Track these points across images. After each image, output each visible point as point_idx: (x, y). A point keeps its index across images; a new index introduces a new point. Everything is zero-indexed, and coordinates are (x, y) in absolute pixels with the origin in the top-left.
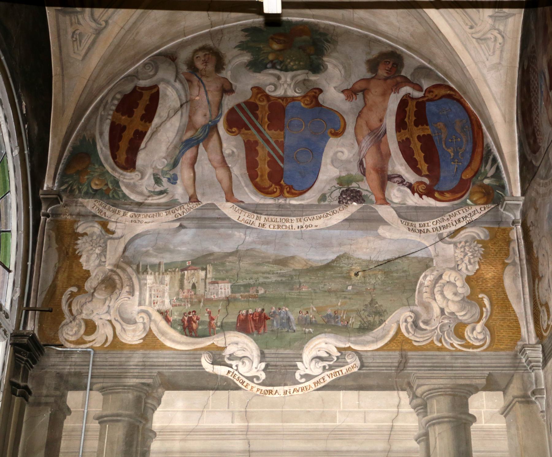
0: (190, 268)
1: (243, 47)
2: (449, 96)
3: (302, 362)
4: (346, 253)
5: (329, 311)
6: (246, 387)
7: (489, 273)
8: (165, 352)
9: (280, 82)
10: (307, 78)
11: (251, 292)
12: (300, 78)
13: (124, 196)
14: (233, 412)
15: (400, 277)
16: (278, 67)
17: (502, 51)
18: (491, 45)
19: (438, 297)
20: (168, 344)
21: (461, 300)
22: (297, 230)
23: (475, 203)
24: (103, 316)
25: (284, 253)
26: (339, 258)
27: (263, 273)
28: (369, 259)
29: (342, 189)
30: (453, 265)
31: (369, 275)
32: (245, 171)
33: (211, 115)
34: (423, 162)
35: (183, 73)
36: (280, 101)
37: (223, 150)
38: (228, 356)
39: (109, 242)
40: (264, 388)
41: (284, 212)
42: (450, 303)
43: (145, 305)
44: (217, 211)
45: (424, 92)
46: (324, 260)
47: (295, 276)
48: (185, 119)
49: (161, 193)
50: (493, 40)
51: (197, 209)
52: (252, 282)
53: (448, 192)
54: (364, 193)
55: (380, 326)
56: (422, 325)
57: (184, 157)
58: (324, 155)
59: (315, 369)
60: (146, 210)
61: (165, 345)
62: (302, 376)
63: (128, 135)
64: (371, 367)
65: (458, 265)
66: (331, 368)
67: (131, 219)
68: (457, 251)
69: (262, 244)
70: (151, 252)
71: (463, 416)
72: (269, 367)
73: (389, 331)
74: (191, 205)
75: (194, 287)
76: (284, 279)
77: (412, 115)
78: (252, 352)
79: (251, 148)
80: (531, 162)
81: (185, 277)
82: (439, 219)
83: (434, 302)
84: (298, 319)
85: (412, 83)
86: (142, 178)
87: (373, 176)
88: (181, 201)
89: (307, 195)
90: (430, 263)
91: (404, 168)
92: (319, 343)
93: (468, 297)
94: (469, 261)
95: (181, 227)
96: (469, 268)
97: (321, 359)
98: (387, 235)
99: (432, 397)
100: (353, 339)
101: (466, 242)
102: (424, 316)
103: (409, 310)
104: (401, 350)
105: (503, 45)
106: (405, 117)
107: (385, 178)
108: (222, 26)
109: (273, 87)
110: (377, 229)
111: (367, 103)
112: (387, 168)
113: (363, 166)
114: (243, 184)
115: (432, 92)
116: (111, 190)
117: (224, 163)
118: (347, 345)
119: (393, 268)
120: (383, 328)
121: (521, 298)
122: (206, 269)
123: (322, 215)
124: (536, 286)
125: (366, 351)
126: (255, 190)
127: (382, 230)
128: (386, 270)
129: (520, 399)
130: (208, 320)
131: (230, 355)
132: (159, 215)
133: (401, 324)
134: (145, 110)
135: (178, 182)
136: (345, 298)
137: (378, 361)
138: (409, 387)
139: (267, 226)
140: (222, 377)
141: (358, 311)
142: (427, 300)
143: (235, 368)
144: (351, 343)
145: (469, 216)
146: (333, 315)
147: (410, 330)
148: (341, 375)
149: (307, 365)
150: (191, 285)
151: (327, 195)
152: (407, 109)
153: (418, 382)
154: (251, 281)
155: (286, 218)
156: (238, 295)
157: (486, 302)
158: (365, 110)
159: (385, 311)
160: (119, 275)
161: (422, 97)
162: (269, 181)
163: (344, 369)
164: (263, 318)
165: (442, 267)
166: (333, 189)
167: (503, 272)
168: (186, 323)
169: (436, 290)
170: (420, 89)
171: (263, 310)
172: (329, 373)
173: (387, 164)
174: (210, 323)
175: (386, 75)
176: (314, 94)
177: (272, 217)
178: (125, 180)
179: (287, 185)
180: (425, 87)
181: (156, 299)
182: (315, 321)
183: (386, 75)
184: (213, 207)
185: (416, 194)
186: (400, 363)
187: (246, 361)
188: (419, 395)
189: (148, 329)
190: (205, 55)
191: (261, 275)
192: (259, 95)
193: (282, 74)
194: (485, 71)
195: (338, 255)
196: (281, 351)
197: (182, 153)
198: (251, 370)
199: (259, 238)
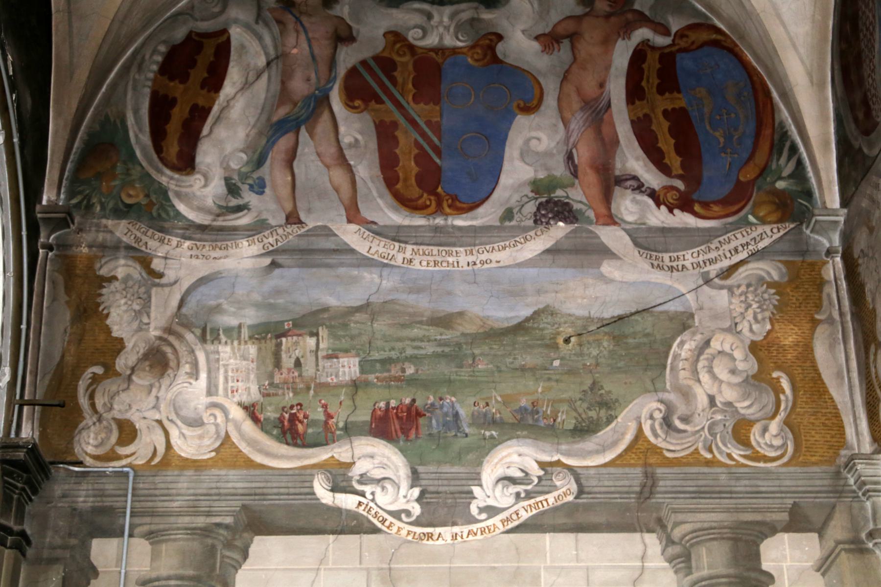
0: (290, 333)
2: (715, 43)
3: (481, 486)
4: (548, 306)
5: (524, 402)
6: (388, 528)
7: (789, 337)
9: (432, 23)
10: (476, 16)
11: (393, 372)
12: (465, 16)
14: (368, 570)
15: (641, 344)
19: (705, 377)
20: (259, 459)
21: (743, 381)
22: (466, 268)
23: (763, 221)
24: (147, 414)
25: (447, 307)
26: (537, 313)
27: (413, 340)
28: (587, 315)
29: (540, 200)
30: (727, 324)
31: (589, 343)
32: (377, 171)
33: (318, 79)
34: (673, 154)
36: (432, 54)
37: (340, 137)
38: (358, 478)
39: (154, 291)
40: (419, 530)
41: (445, 239)
42: (724, 386)
44: (333, 238)
45: (672, 38)
46: (512, 318)
47: (466, 343)
48: (276, 87)
49: (239, 209)
51: (299, 236)
52: (394, 354)
53: (716, 203)
54: (576, 206)
55: (608, 425)
56: (678, 424)
57: (275, 148)
58: (507, 143)
59: (503, 497)
60: (214, 237)
61: (252, 461)
62: (481, 510)
63: (179, 114)
64: (596, 493)
65: (736, 324)
66: (529, 495)
68: (734, 301)
69: (410, 293)
70: (225, 306)
71: (753, 575)
72: (427, 496)
73: (623, 434)
74: (289, 229)
75: (298, 364)
76: (447, 350)
77: (654, 75)
78: (398, 471)
79: (385, 134)
80: (860, 149)
81: (283, 347)
82: (703, 247)
83: (698, 384)
84: (473, 415)
86: (205, 186)
87: (590, 177)
88: (272, 222)
89: (481, 210)
90: (690, 322)
91: (641, 163)
92: (509, 455)
93: (754, 377)
94: (755, 318)
95: (274, 265)
96: (755, 328)
97: (512, 481)
98: (617, 275)
99: (698, 543)
100: (564, 447)
101: (748, 286)
102: (682, 409)
103: (656, 398)
104: (646, 465)
106: (642, 79)
107: (610, 182)
109: (420, 31)
110: (599, 265)
111: (577, 56)
112: (614, 165)
113: (573, 161)
114: (375, 194)
115: (687, 36)
116: (154, 204)
118: (555, 458)
119: (628, 330)
120: (614, 430)
121: (843, 378)
122: (317, 335)
123: (507, 243)
124: (872, 357)
125: (587, 467)
127: (607, 268)
128: (617, 333)
129: (847, 546)
130: (322, 417)
131: (362, 475)
132: (237, 246)
133: (643, 421)
134: (208, 73)
135: (267, 190)
136: (549, 379)
137: (606, 483)
138: (659, 525)
139: (416, 262)
141: (571, 402)
142: (686, 382)
143: (371, 497)
144: (562, 454)
145: (753, 243)
146: (530, 408)
147: (659, 431)
148: (546, 507)
149: (488, 492)
150: (293, 360)
151: (515, 211)
152: (645, 66)
153: (673, 518)
154: (393, 353)
155: (447, 249)
156: (371, 377)
157: (785, 384)
158: (575, 68)
159: (617, 401)
162: (417, 189)
163: (551, 498)
164: (414, 413)
165: (709, 327)
166: (525, 199)
168: (286, 423)
169: (700, 365)
170: (666, 32)
171: (414, 401)
172: (525, 503)
173: (614, 158)
174: (326, 423)
175: (608, 9)
176: (489, 43)
177: (425, 247)
179: (448, 195)
180: (674, 29)
181: (235, 384)
182: (501, 418)
183: (608, 9)
184: (326, 232)
185: (663, 207)
186: (643, 486)
188: (676, 540)
189: (223, 434)
191: (409, 343)
192: (398, 45)
195: (536, 308)
196: (446, 468)
197: (271, 142)
198: (395, 500)
199: (404, 283)
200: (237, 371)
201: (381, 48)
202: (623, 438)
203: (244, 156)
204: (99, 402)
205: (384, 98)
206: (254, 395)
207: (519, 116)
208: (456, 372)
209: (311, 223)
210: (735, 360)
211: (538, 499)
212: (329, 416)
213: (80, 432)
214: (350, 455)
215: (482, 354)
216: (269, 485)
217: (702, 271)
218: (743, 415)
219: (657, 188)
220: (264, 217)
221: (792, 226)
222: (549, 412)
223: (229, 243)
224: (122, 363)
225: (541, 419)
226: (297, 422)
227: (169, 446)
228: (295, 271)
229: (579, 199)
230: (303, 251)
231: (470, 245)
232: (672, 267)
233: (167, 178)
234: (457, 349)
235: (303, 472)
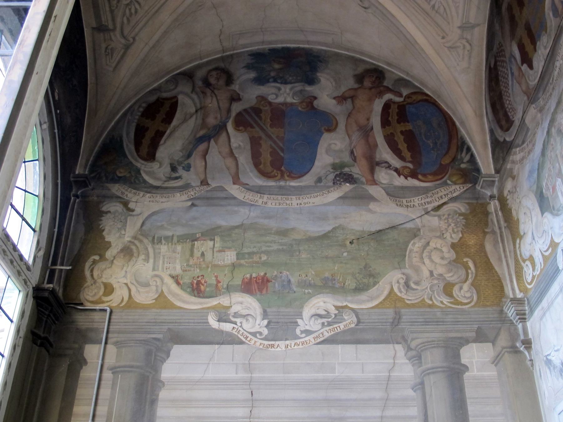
1: (249, 67)
3: (302, 319)
4: (341, 225)
5: (327, 275)
6: (249, 341)
7: (472, 241)
8: (175, 311)
13: (145, 181)
16: (279, 81)
17: (470, 57)
19: (427, 261)
20: (179, 304)
22: (296, 206)
23: (455, 183)
24: (120, 280)
27: (266, 242)
30: (438, 234)
33: (221, 118)
34: (406, 151)
36: (281, 106)
37: (231, 144)
40: (266, 343)
41: (284, 192)
43: (158, 270)
48: (200, 121)
49: (176, 178)
50: (462, 47)
51: (207, 191)
52: (255, 250)
53: (430, 174)
54: (355, 176)
56: (413, 285)
57: (197, 149)
59: (315, 325)
61: (175, 305)
62: (302, 332)
66: (329, 324)
67: (150, 199)
68: (441, 222)
70: (165, 226)
73: (383, 291)
74: (202, 188)
75: (203, 254)
76: (285, 247)
78: (256, 311)
80: (505, 140)
81: (195, 246)
82: (424, 196)
86: (160, 167)
87: (363, 163)
88: (193, 184)
89: (305, 178)
90: (418, 233)
92: (318, 302)
93: (454, 261)
94: (453, 231)
95: (193, 205)
97: (320, 316)
98: (378, 209)
99: (426, 349)
100: (349, 298)
101: (449, 215)
102: (414, 277)
108: (232, 52)
113: (354, 155)
114: (248, 170)
115: (411, 97)
117: (231, 154)
118: (345, 304)
121: (501, 261)
122: (214, 240)
123: (319, 194)
124: (517, 246)
126: (259, 175)
127: (372, 206)
130: (215, 283)
131: (235, 313)
135: (191, 169)
136: (341, 263)
137: (373, 317)
138: (404, 340)
140: (227, 332)
143: (240, 325)
144: (348, 302)
146: (330, 277)
147: (402, 290)
149: (306, 322)
150: (200, 253)
151: (323, 178)
154: (255, 249)
157: (471, 264)
159: (379, 274)
161: (402, 102)
163: (342, 326)
164: (265, 280)
168: (195, 285)
169: (424, 255)
170: (400, 95)
171: (266, 274)
172: (327, 328)
174: (217, 285)
175: (370, 85)
177: (274, 196)
178: (146, 169)
180: (404, 94)
181: (168, 265)
183: (370, 85)
184: (222, 189)
185: (402, 176)
186: (394, 319)
187: (250, 318)
189: (160, 291)
190: (217, 74)
192: (263, 102)
193: (282, 87)
195: (334, 226)
196: (283, 309)
197: (195, 147)
198: (253, 327)
203: (181, 154)
204: (96, 274)
205: (255, 125)
209: (214, 184)
210: (443, 252)
212: (219, 282)
213: (84, 289)
214: (229, 302)
216: (184, 318)
220: (189, 182)
221: (470, 185)
223: (170, 195)
224: (109, 254)
227: (130, 296)
228: (203, 208)
230: (208, 198)
231: (299, 195)
233: (139, 164)
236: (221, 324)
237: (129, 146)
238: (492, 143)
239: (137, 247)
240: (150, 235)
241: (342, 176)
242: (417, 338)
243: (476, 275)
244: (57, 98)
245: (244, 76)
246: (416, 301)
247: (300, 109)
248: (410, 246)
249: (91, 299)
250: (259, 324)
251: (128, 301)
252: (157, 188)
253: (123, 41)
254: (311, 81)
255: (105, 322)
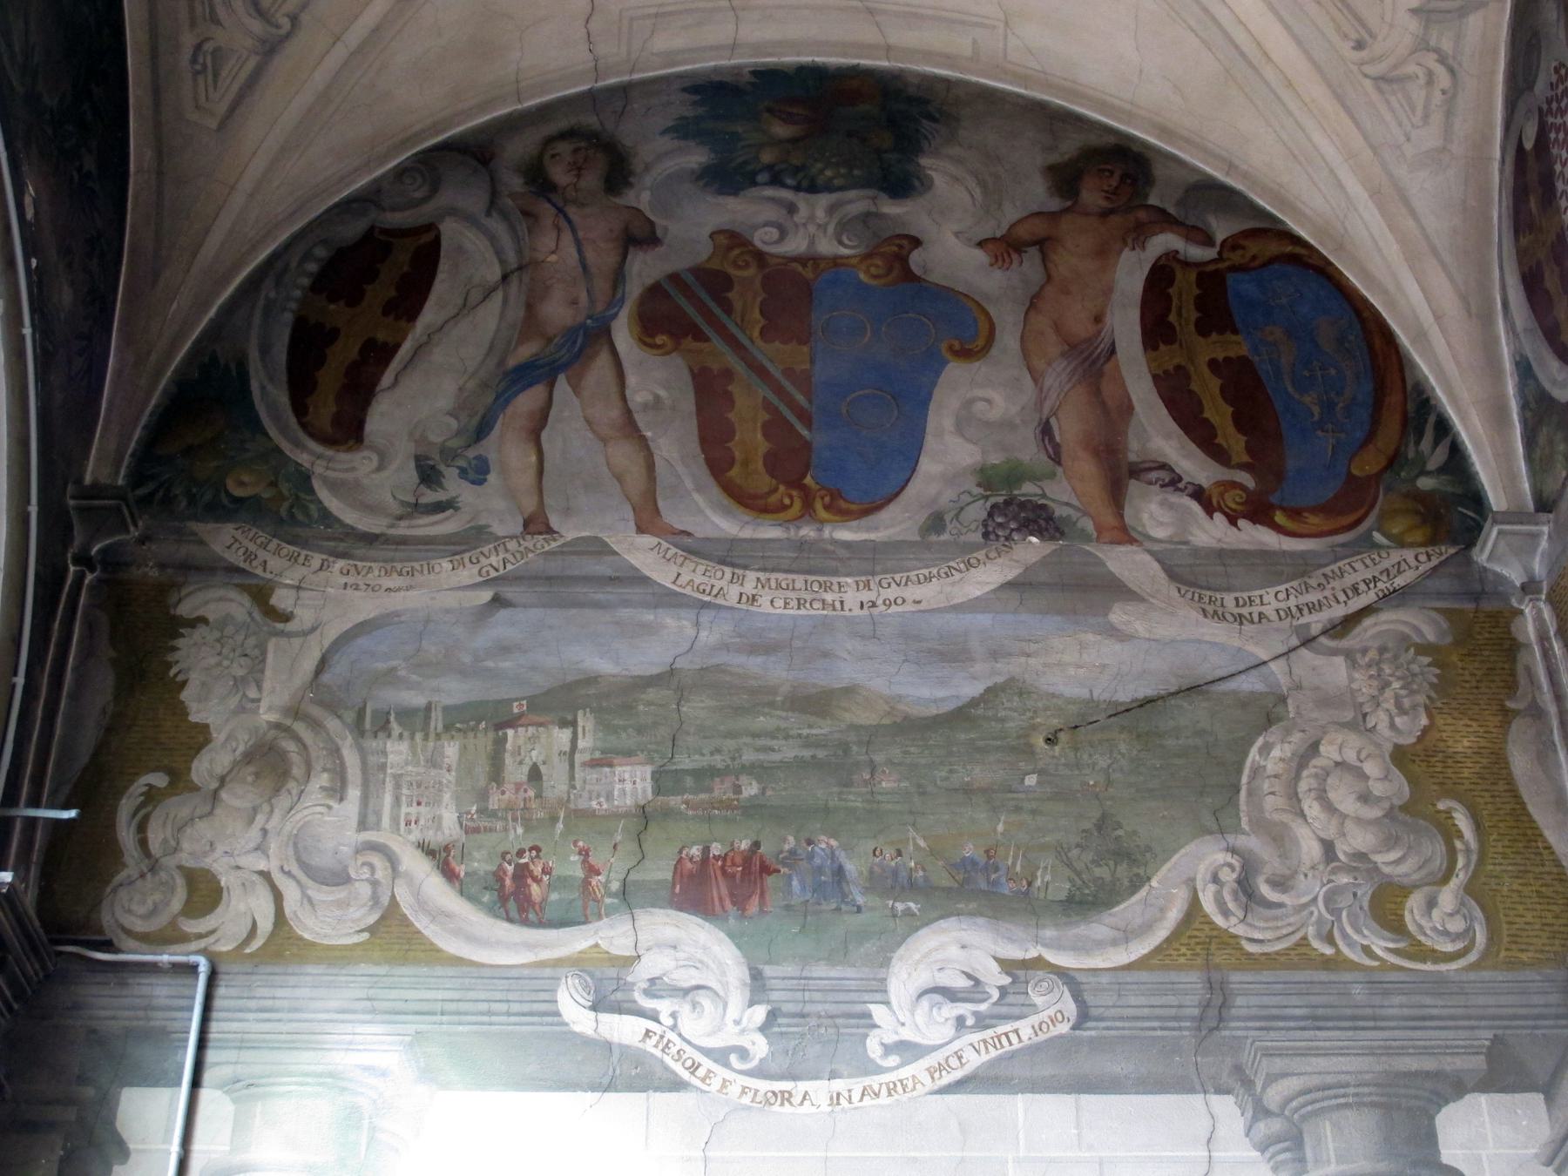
0: (523, 721)
1: (683, 130)
3: (887, 1003)
4: (1012, 679)
5: (969, 851)
6: (703, 1080)
7: (1463, 740)
8: (439, 971)
10: (873, 209)
13: (327, 516)
16: (789, 181)
17: (1449, 114)
18: (1418, 93)
19: (1312, 809)
20: (451, 946)
22: (857, 612)
23: (1401, 544)
24: (243, 861)
25: (819, 678)
26: (992, 692)
27: (755, 735)
28: (1088, 696)
29: (993, 500)
30: (1349, 715)
32: (694, 446)
33: (592, 301)
34: (1231, 429)
35: (512, 195)
37: (628, 392)
38: (645, 985)
40: (764, 1086)
41: (816, 562)
42: (1349, 825)
43: (377, 826)
44: (611, 558)
45: (1218, 248)
46: (943, 700)
48: (516, 313)
49: (439, 507)
50: (1422, 80)
51: (547, 553)
52: (718, 761)
53: (1314, 510)
54: (1060, 512)
55: (1133, 893)
56: (1265, 890)
57: (510, 410)
58: (932, 406)
59: (932, 1025)
60: (390, 554)
61: (439, 950)
62: (888, 1049)
65: (1365, 715)
66: (982, 1022)
67: (344, 580)
68: (1357, 675)
70: (402, 673)
72: (780, 1020)
73: (1163, 910)
74: (529, 542)
75: (535, 775)
76: (821, 754)
78: (724, 973)
81: (509, 746)
82: (1295, 583)
83: (1300, 821)
84: (871, 872)
85: (1182, 224)
86: (380, 469)
87: (1086, 466)
88: (498, 529)
89: (884, 515)
90: (1280, 709)
93: (1404, 808)
94: (1398, 705)
95: (498, 602)
97: (950, 994)
98: (1140, 627)
99: (1315, 1113)
100: (1049, 933)
101: (1382, 650)
102: (1272, 863)
105: (1450, 97)
106: (1169, 310)
108: (626, 78)
110: (1106, 611)
113: (1052, 439)
114: (689, 484)
115: (1243, 248)
116: (284, 499)
117: (629, 426)
118: (1032, 953)
122: (574, 724)
126: (727, 501)
127: (1119, 615)
130: (579, 873)
131: (652, 981)
132: (431, 570)
133: (1199, 886)
135: (492, 478)
136: (1018, 809)
137: (1133, 1001)
138: (1240, 1081)
139: (764, 601)
140: (624, 1048)
142: (1276, 817)
143: (670, 1022)
145: (1384, 578)
146: (982, 860)
147: (1231, 905)
148: (1016, 1045)
150: (526, 769)
151: (948, 518)
154: (718, 757)
155: (821, 579)
157: (1462, 821)
159: (1149, 849)
160: (298, 739)
161: (1213, 261)
162: (767, 478)
163: (1025, 1028)
164: (756, 867)
165: (1316, 720)
166: (966, 498)
167: (1506, 734)
168: (508, 882)
169: (1303, 786)
170: (1208, 241)
171: (756, 845)
172: (976, 1037)
174: (586, 883)
175: (1104, 204)
176: (897, 253)
177: (781, 576)
178: (330, 473)
179: (823, 488)
180: (1220, 237)
181: (414, 810)
182: (926, 879)
183: (1104, 204)
184: (599, 548)
185: (1218, 516)
186: (1206, 1006)
187: (705, 1001)
188: (1273, 1107)
189: (385, 900)
190: (576, 151)
191: (748, 740)
192: (736, 252)
193: (802, 201)
194: (1401, 172)
195: (990, 683)
196: (820, 970)
197: (503, 399)
200: (419, 786)
201: (705, 256)
202: (1162, 918)
203: (454, 424)
204: (157, 836)
206: (449, 824)
207: (950, 366)
208: (840, 793)
210: (1367, 778)
211: (1001, 1029)
212: (593, 871)
213: (115, 891)
214: (630, 942)
215: (890, 762)
217: (1295, 623)
218: (1388, 876)
219: (1205, 483)
220: (482, 522)
221: (1452, 551)
222: (1018, 868)
223: (417, 565)
224: (204, 768)
225: (1003, 880)
226: (529, 881)
228: (535, 613)
229: (1065, 499)
230: (549, 579)
231: (865, 574)
232: (1240, 616)
233: (308, 455)
234: (840, 752)
235: (538, 972)
236: (605, 1018)
237: (269, 392)
238: (1524, 407)
239: (305, 746)
240: (350, 707)
241: (1014, 511)
242: (1285, 1075)
243: (1481, 861)
244: (30, 214)
245: (666, 161)
246: (1279, 947)
247: (862, 276)
248: (1253, 753)
249: (139, 926)
250: (736, 1021)
251: (273, 934)
252: (370, 539)
253: (256, 26)
254: (901, 184)
255: (191, 1009)
